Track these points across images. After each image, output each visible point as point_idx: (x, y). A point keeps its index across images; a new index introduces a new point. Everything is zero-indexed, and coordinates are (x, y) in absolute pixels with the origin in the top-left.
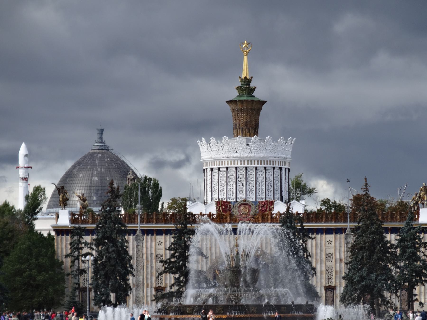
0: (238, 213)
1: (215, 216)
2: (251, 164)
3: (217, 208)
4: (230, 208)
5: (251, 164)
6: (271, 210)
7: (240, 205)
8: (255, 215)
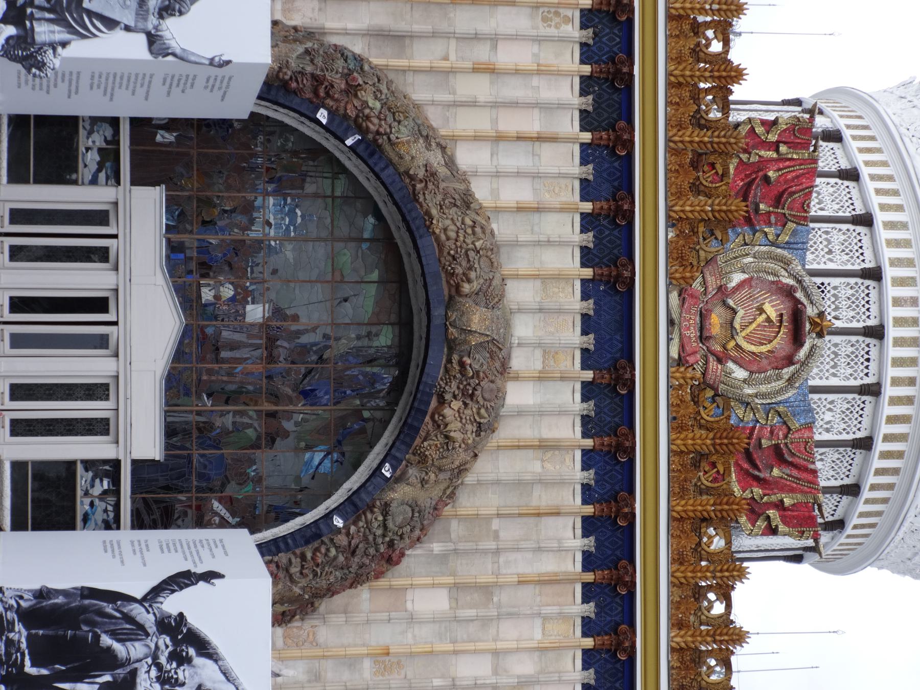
0: (737, 278)
1: (715, 115)
2: (898, 362)
3: (770, 125)
5: (898, 362)
6: (755, 511)
7: (788, 293)
8: (723, 400)
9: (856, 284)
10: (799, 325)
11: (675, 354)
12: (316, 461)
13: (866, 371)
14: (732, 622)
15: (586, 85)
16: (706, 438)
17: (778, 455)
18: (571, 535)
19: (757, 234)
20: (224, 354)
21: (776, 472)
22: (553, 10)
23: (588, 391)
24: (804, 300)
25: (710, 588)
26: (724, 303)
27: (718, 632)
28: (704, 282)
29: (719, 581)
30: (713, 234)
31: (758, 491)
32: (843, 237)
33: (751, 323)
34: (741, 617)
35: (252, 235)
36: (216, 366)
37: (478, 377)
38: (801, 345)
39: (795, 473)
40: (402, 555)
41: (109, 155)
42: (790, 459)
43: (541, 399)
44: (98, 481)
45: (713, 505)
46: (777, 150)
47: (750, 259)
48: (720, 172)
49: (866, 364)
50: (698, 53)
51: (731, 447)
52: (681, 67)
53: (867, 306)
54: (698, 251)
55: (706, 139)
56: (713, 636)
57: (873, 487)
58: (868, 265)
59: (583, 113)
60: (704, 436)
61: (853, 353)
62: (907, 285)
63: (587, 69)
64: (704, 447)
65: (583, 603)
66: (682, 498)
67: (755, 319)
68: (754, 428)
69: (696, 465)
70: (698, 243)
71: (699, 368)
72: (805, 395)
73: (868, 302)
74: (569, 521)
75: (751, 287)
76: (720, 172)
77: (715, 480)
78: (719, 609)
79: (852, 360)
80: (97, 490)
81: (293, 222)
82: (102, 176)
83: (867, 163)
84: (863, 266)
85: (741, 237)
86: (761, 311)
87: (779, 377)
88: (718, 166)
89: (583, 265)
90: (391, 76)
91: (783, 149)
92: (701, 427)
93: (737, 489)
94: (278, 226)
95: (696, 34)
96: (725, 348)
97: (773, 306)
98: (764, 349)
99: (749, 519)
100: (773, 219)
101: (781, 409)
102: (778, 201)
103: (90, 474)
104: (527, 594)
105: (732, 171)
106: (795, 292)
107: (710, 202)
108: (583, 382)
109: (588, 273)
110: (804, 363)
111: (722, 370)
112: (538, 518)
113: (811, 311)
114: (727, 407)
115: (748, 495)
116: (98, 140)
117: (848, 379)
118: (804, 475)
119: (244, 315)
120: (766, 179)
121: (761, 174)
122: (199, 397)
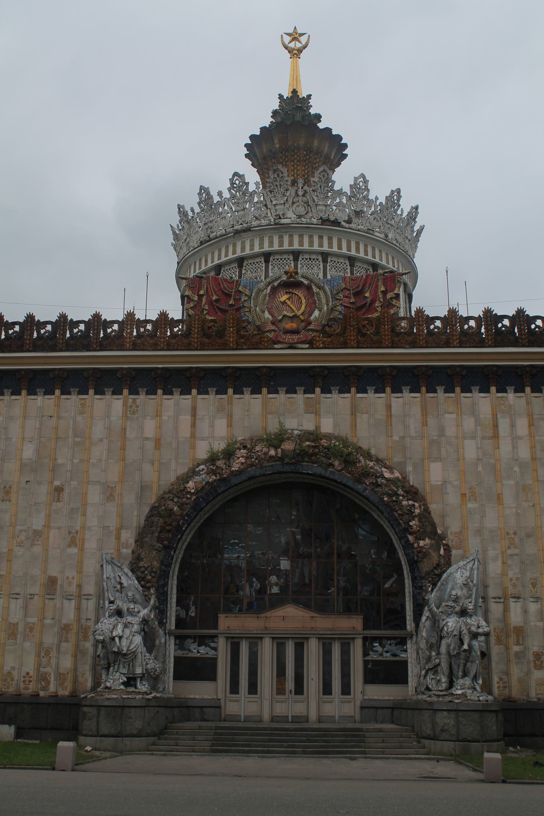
0: (267, 315)
2: (311, 244)
4: (237, 300)
5: (311, 244)
6: (388, 305)
7: (274, 290)
8: (330, 322)
9: (272, 265)
10: (291, 284)
11: (307, 346)
12: (364, 533)
13: (316, 260)
14: (445, 316)
15: (168, 392)
16: (350, 329)
17: (359, 294)
18: (401, 400)
19: (245, 305)
20: (307, 581)
21: (367, 295)
22: (129, 409)
23: (326, 390)
24: (278, 282)
25: (428, 328)
26: (280, 321)
27: (451, 323)
28: (270, 331)
29: (424, 323)
30: (245, 328)
31: (377, 304)
32: (249, 272)
33: (291, 308)
34: (443, 313)
35: (244, 566)
36: (313, 585)
37: (319, 446)
38: (302, 282)
39: (367, 285)
40: (413, 486)
41: (202, 640)
42: (360, 288)
43: (331, 415)
44: (374, 649)
45: (385, 326)
46: (202, 296)
47: (258, 309)
48: (213, 324)
49: (312, 260)
50: (152, 335)
51: (355, 317)
52: (159, 343)
53: (283, 260)
54: (254, 335)
55: (196, 331)
56: (453, 325)
57: (374, 257)
58: (263, 260)
59: (182, 393)
60: (349, 330)
61: (307, 266)
62: (273, 240)
63: (160, 392)
64: (355, 331)
65: (437, 393)
66: (382, 342)
67: (289, 306)
68: (345, 306)
69: (364, 335)
70: (250, 334)
71: (314, 334)
72: (328, 281)
73: (281, 259)
74: (393, 400)
75: (272, 308)
76: (213, 324)
77: (372, 325)
78: (438, 323)
79: (310, 266)
80: (380, 649)
81: (237, 544)
82: (212, 645)
83: (212, 262)
84: (263, 261)
85: (247, 313)
86: (284, 303)
87: (318, 294)
88: (210, 325)
89: (260, 393)
90: (161, 492)
91: (202, 292)
92: (344, 333)
93: (376, 315)
94: (239, 552)
95: (143, 336)
96: (302, 321)
97: (282, 297)
98: (304, 301)
99: (392, 308)
100: (238, 297)
101: (335, 292)
102: (228, 296)
103: (371, 653)
104: (431, 421)
105: (213, 318)
106: (274, 286)
107: (228, 329)
108: (321, 393)
109: (265, 390)
110: (311, 281)
111: (315, 322)
112: (393, 417)
113: (284, 278)
114: (334, 319)
115: (379, 309)
116: (193, 647)
117: (320, 268)
118: (369, 282)
119: (286, 571)
120: (217, 301)
121: (214, 303)
122: (330, 594)
